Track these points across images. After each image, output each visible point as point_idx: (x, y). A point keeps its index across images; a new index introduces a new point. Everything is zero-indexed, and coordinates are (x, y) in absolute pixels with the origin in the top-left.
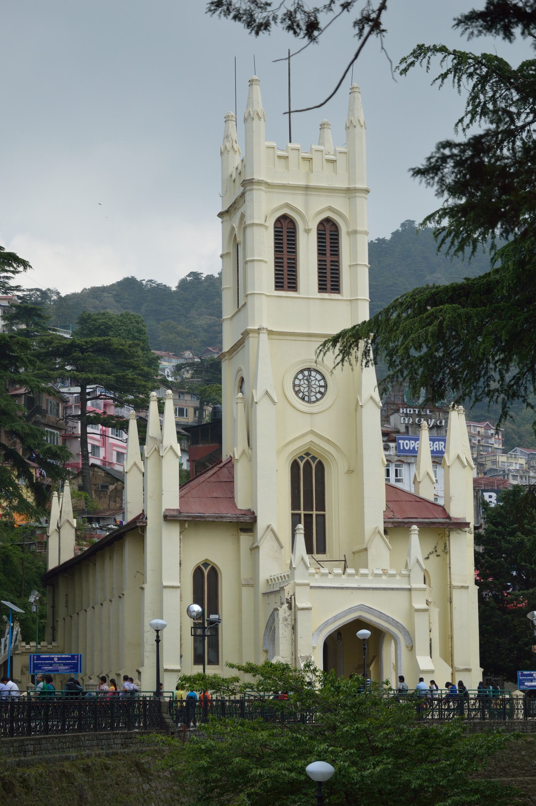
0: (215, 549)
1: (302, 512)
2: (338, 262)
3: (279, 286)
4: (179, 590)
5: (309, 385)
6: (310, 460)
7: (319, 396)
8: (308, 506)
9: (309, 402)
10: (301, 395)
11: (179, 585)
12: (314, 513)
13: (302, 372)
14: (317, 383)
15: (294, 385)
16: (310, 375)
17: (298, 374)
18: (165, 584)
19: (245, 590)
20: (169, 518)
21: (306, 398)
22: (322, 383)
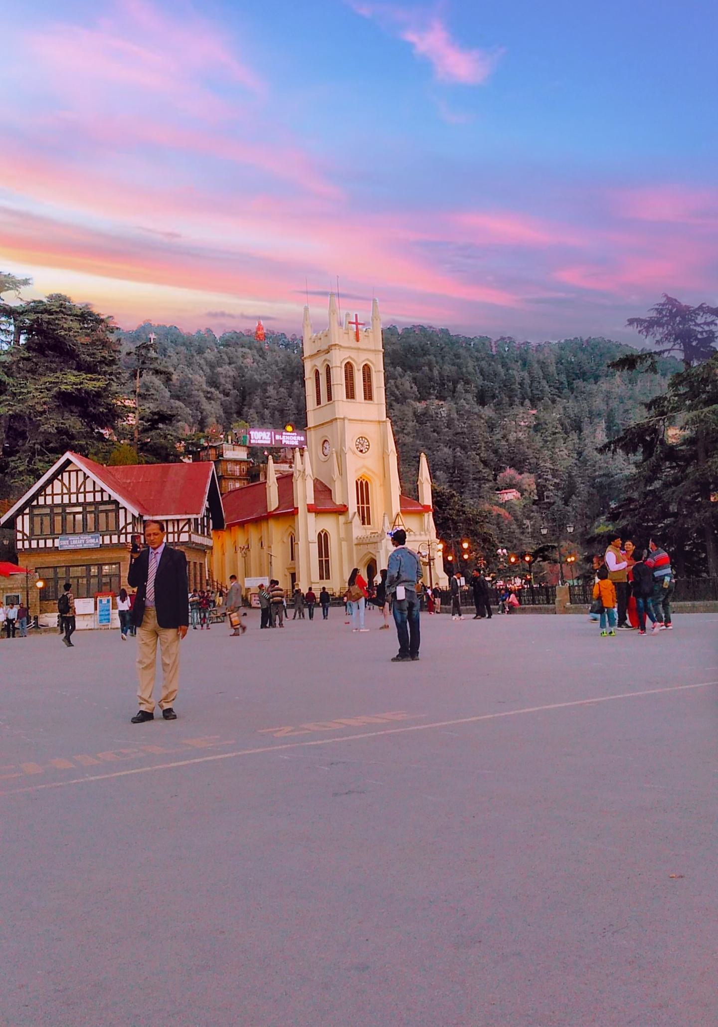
3: (347, 397)
5: (362, 446)
8: (363, 503)
12: (365, 506)
19: (344, 543)
20: (311, 509)
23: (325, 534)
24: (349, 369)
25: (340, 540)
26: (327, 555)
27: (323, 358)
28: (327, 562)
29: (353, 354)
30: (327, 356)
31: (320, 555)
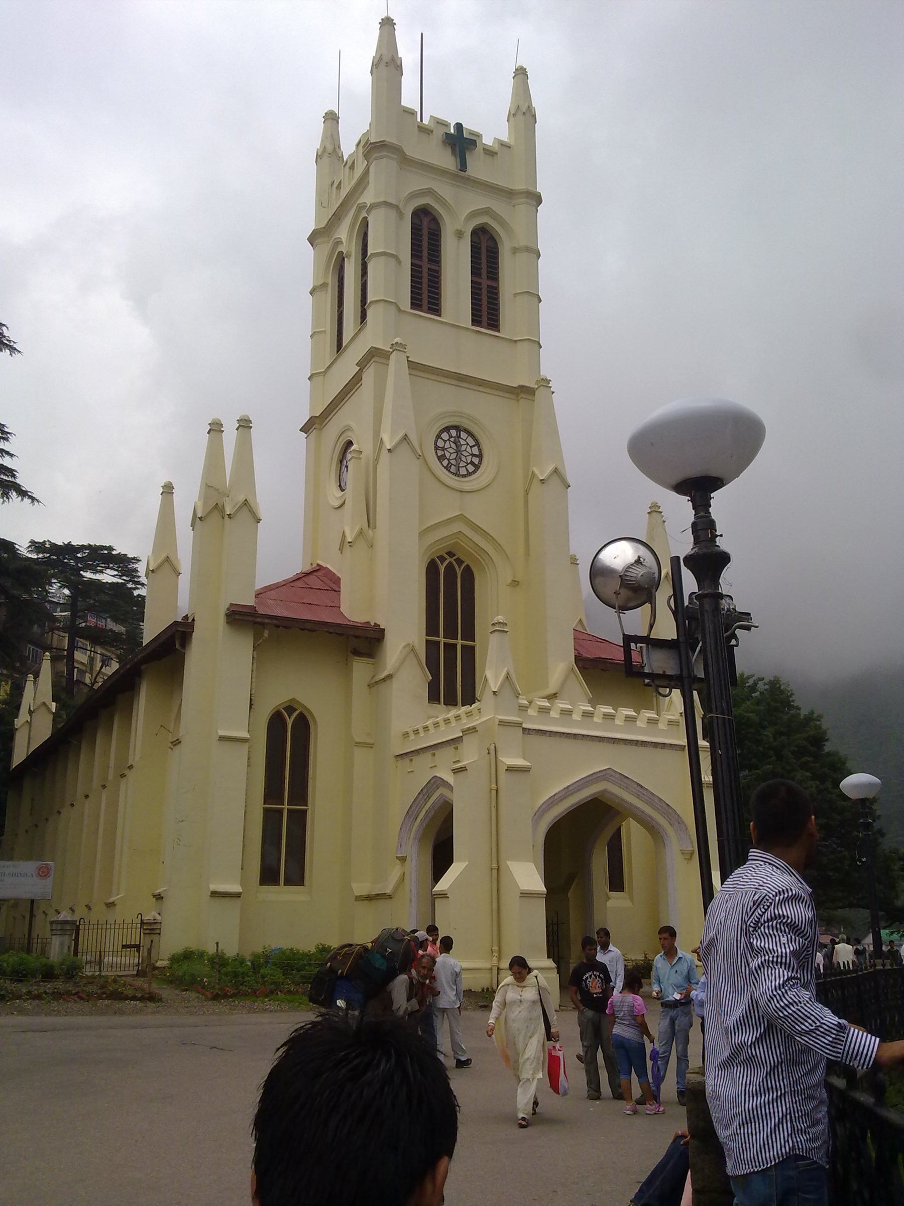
0: (307, 685)
1: (442, 640)
2: (497, 288)
4: (246, 746)
6: (454, 563)
7: (471, 468)
8: (451, 632)
9: (457, 474)
10: (445, 463)
11: (246, 735)
12: (460, 642)
13: (447, 429)
14: (469, 449)
15: (437, 448)
16: (459, 437)
17: (442, 431)
19: (359, 753)
21: (453, 469)
22: (475, 451)
26: (300, 793)
28: (299, 820)
29: (445, 190)
31: (272, 792)
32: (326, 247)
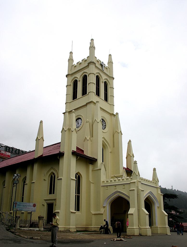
18: (72, 178)
23: (79, 176)
24: (98, 79)
25: (89, 183)
27: (82, 72)
30: (85, 71)
32: (71, 78)
